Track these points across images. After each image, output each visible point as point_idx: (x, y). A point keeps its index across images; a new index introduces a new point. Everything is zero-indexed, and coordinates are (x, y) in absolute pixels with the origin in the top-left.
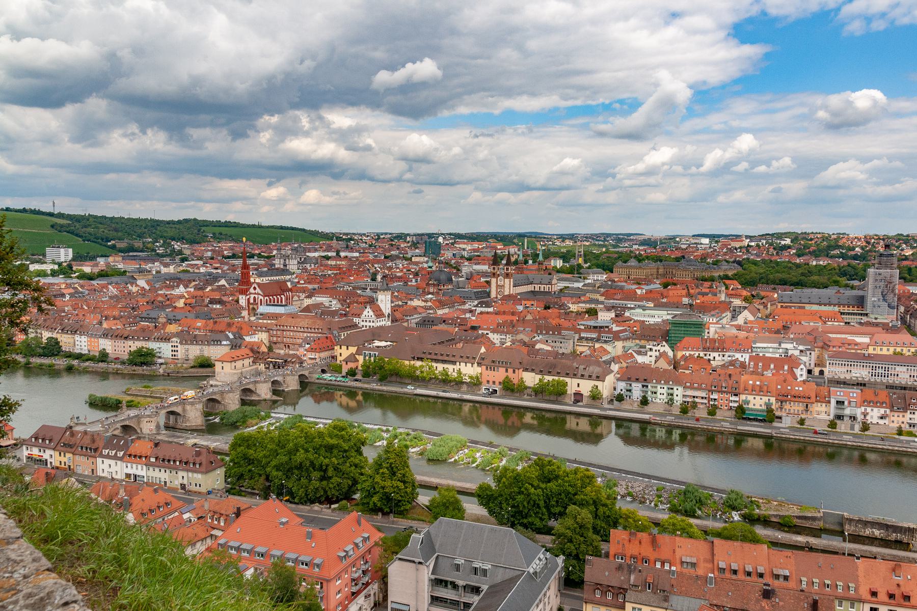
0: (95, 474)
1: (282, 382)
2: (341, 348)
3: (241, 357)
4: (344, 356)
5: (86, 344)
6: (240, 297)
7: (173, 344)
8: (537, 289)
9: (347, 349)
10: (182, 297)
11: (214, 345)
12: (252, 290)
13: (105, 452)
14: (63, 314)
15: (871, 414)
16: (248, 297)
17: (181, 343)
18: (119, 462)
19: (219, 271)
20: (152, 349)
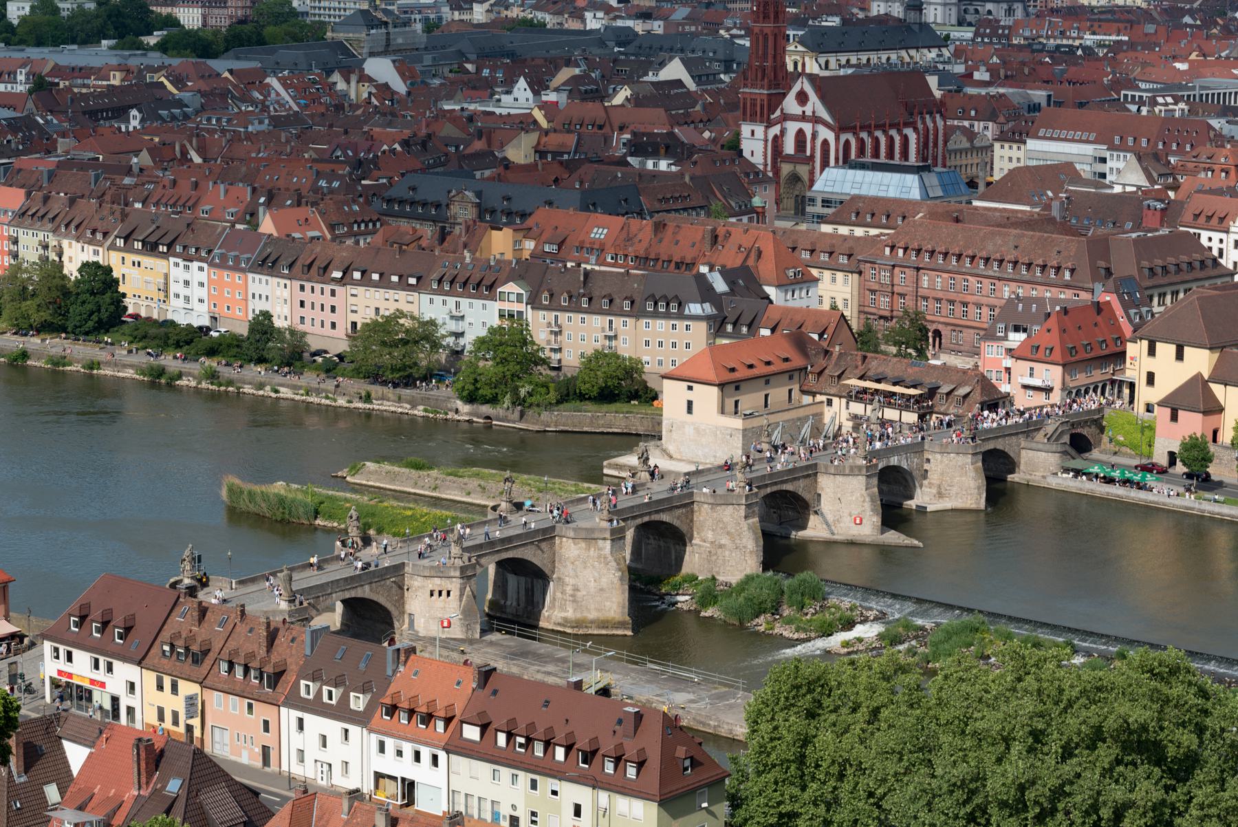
0: (274, 767)
2: (1152, 352)
3: (761, 370)
4: (1169, 382)
5: (203, 292)
6: (746, 129)
7: (507, 306)
9: (1180, 356)
10: (525, 123)
12: (790, 104)
13: (308, 689)
14: (127, 181)
16: (776, 130)
17: (534, 302)
18: (355, 730)
19: (657, 27)
20: (432, 323)
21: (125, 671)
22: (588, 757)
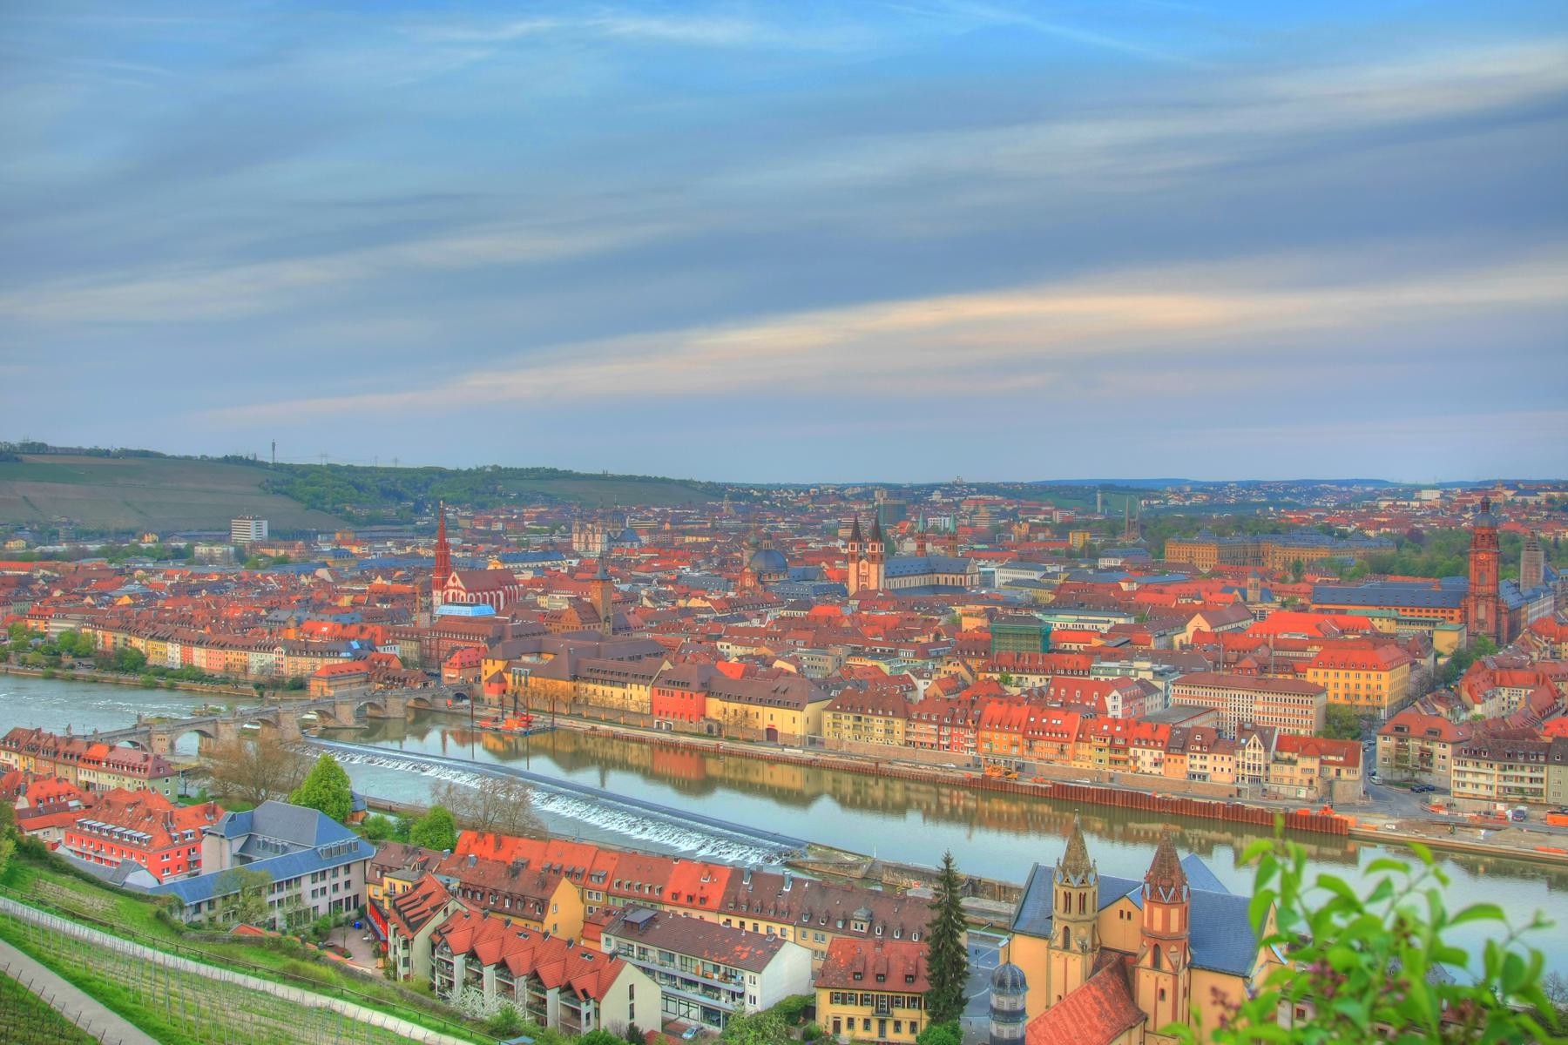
1: (382, 706)
8: (942, 582)
11: (329, 657)
12: (450, 583)
14: (167, 615)
15: (1143, 759)
16: (445, 593)
17: (288, 654)
21: (15, 756)
22: (134, 769)
